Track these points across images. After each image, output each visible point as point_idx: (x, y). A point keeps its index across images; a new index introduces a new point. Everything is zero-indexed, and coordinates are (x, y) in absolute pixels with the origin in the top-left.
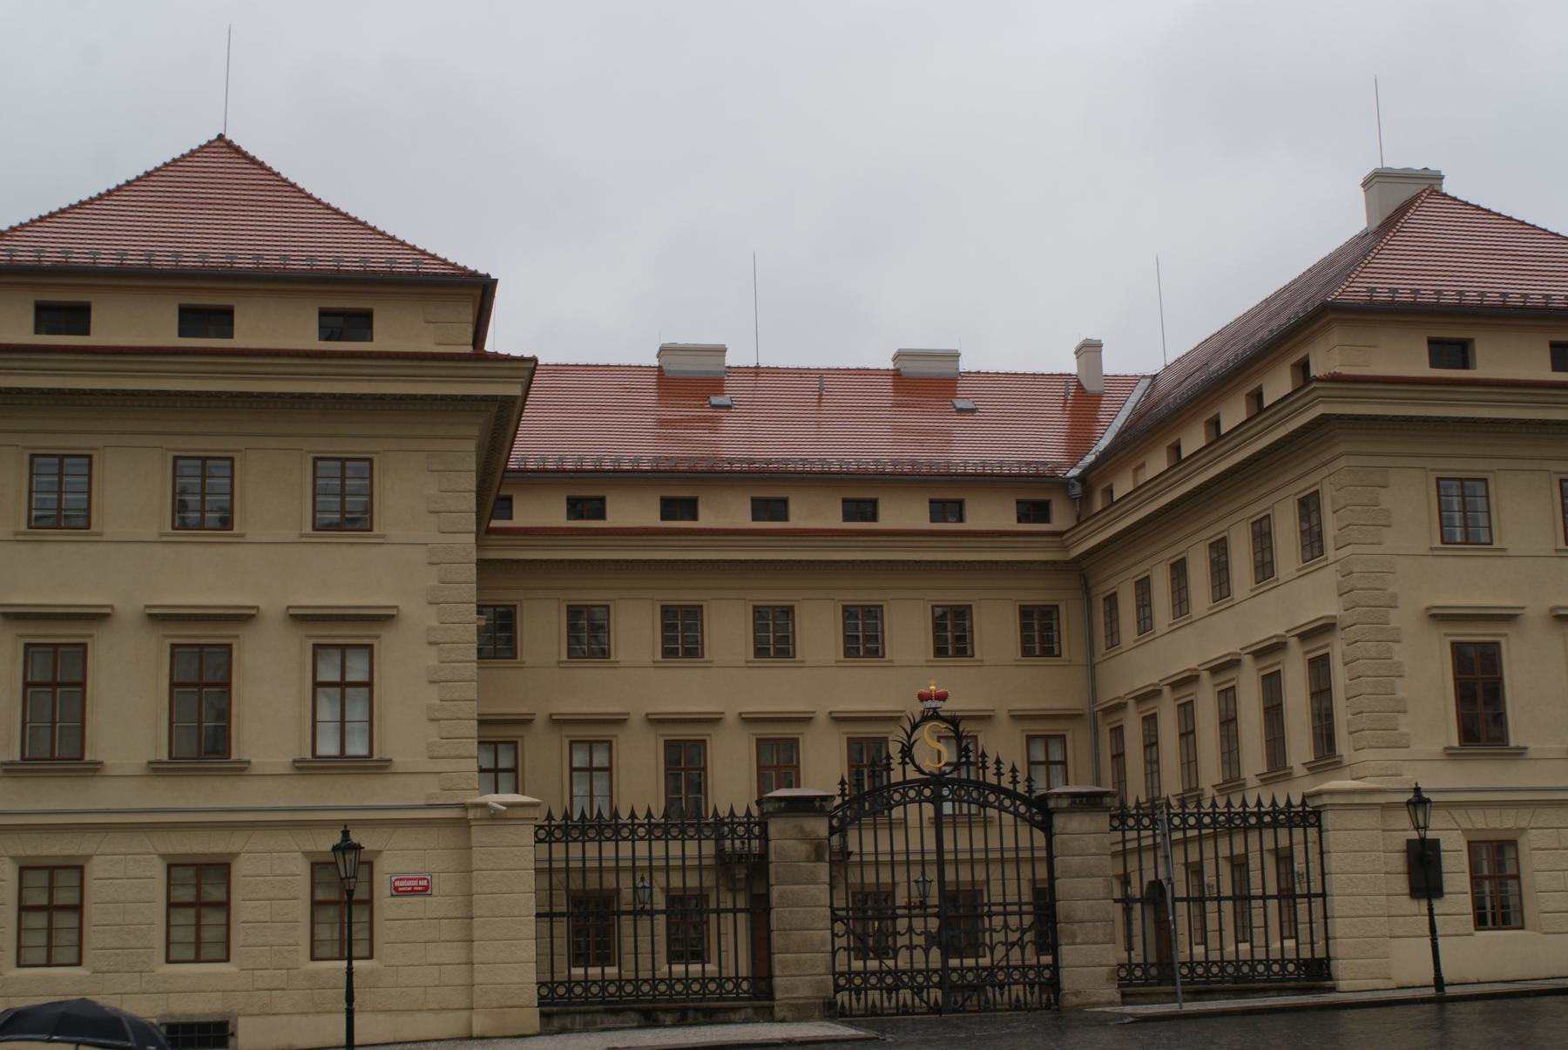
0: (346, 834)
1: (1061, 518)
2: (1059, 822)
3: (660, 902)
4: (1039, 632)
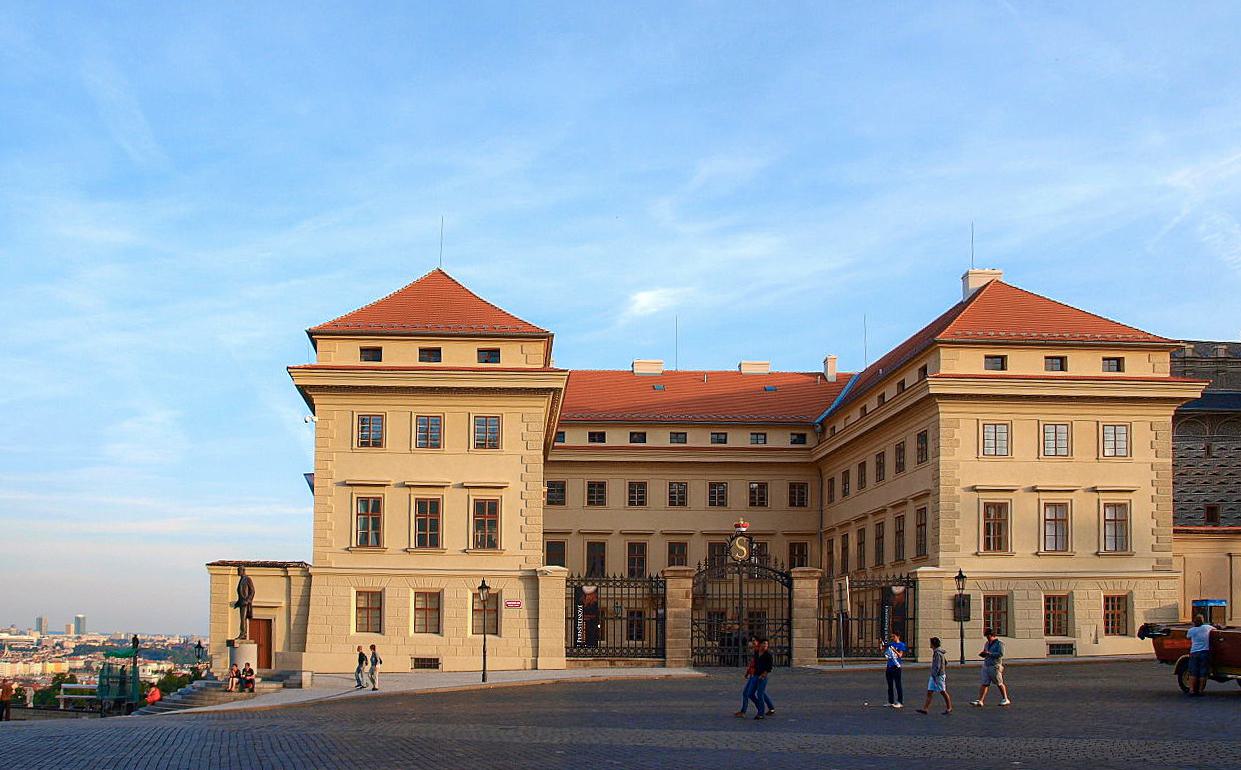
0: (483, 581)
1: (811, 441)
2: (796, 582)
3: (625, 616)
4: (798, 496)
